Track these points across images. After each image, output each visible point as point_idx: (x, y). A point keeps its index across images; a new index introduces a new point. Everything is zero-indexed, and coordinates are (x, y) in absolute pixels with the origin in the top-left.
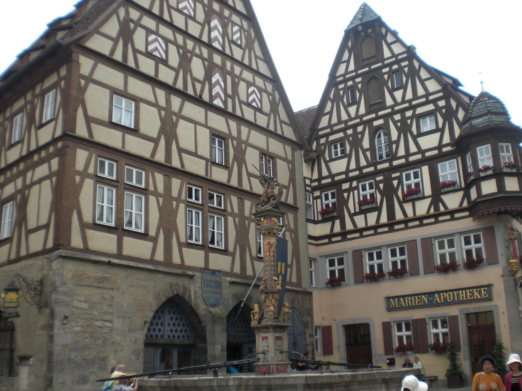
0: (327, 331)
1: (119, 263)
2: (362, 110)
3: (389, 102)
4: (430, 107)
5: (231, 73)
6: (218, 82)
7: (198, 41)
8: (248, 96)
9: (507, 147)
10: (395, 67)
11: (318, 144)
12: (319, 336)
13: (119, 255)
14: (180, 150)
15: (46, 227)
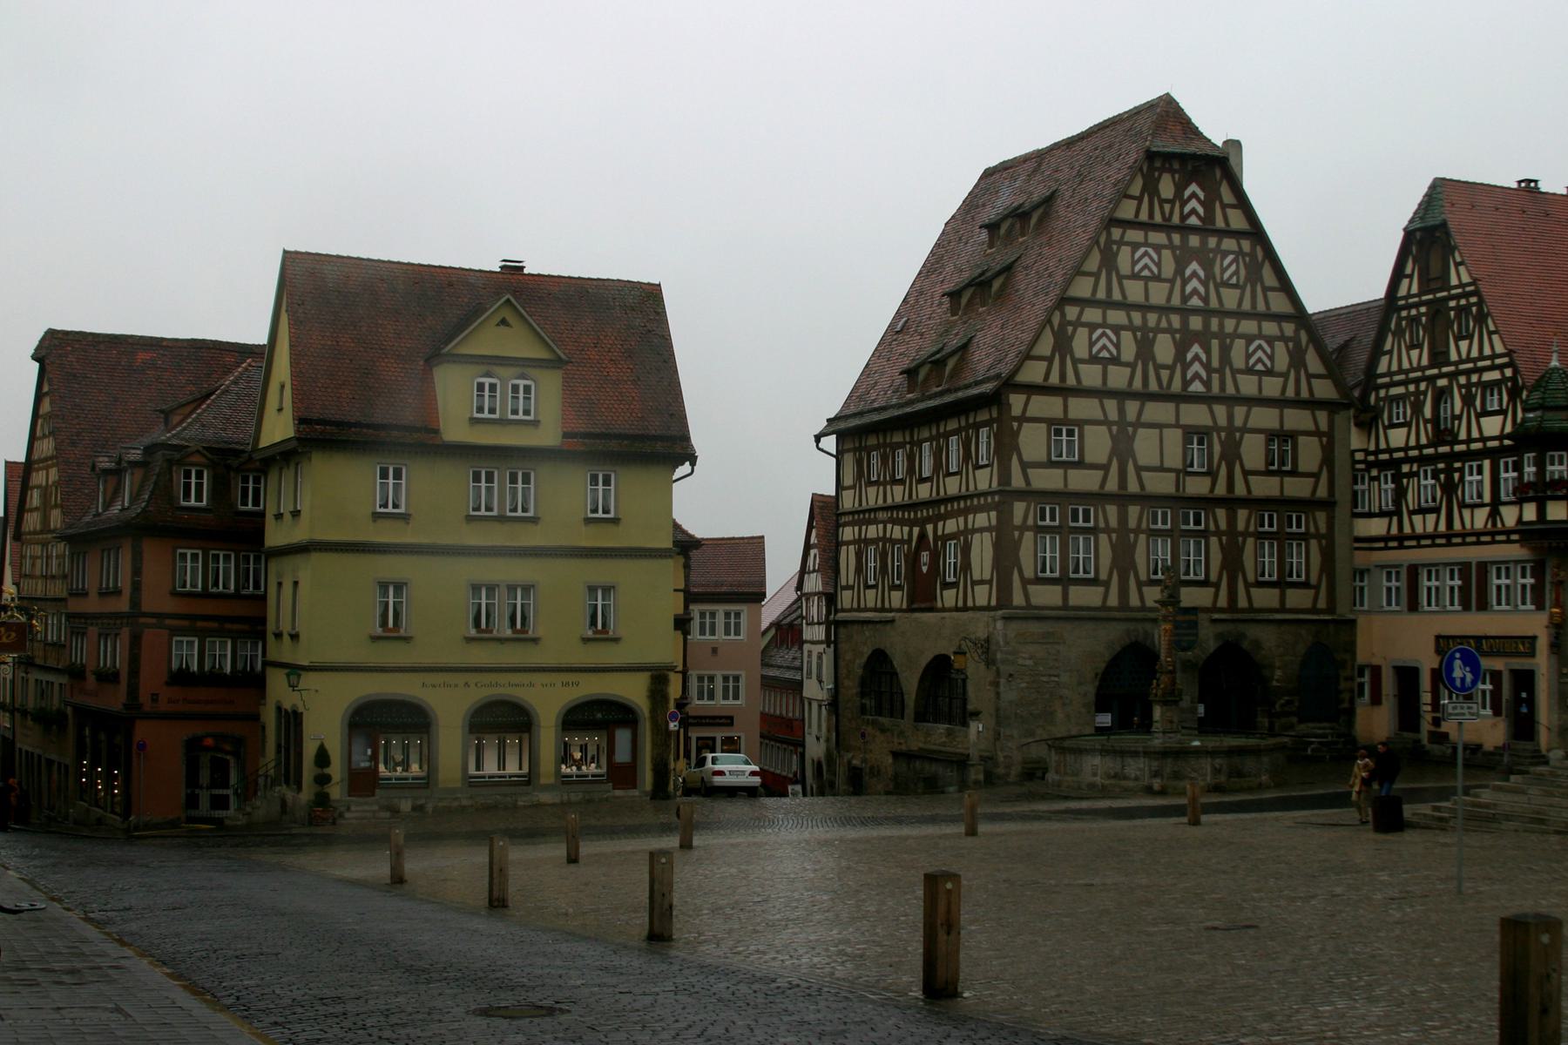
0: (1376, 671)
1: (1069, 615)
2: (1425, 362)
3: (1454, 356)
4: (1495, 375)
5: (1221, 335)
6: (1196, 358)
7: (1164, 310)
8: (1248, 356)
9: (1561, 457)
10: (1463, 302)
11: (1378, 398)
12: (1366, 679)
13: (1065, 607)
14: (1139, 469)
15: (990, 582)
